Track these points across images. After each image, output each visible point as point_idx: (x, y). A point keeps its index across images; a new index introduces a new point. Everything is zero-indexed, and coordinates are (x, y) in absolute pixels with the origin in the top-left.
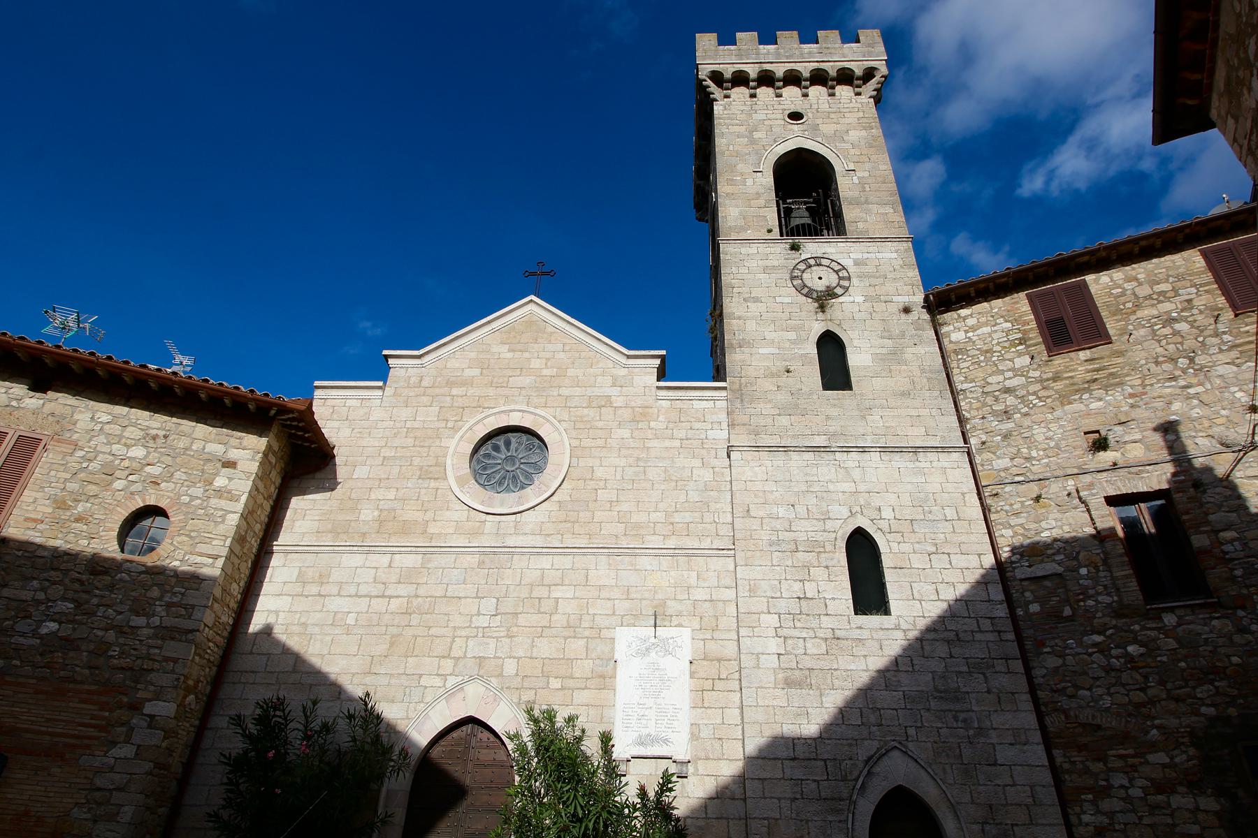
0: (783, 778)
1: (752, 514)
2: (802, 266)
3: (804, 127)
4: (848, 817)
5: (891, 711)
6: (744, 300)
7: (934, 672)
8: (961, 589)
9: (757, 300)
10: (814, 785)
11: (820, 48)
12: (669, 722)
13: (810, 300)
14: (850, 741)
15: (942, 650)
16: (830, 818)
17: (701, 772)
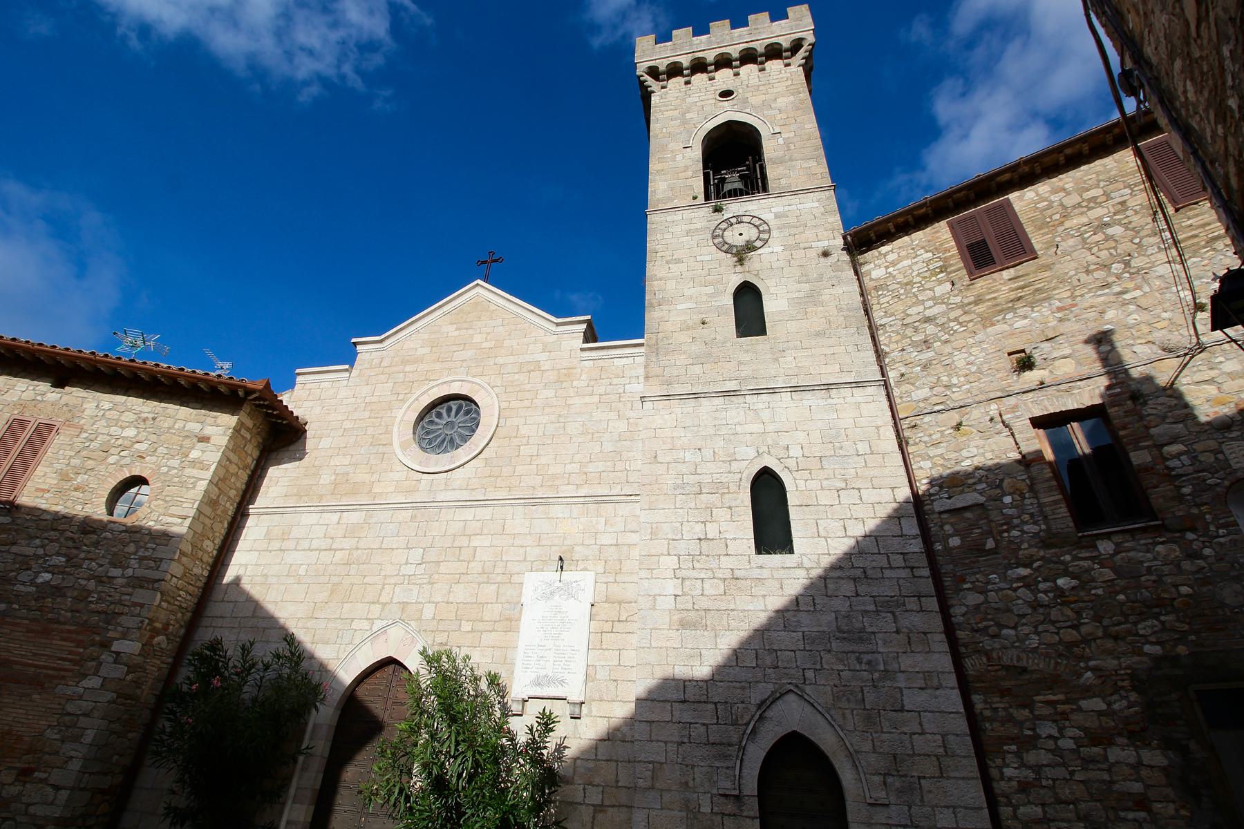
0: (671, 721)
1: (659, 459)
3: (734, 102)
5: (789, 653)
6: (667, 262)
8: (871, 525)
9: (679, 261)
10: (703, 729)
13: (729, 255)
14: (743, 684)
15: (848, 588)
16: (718, 765)
17: (594, 713)
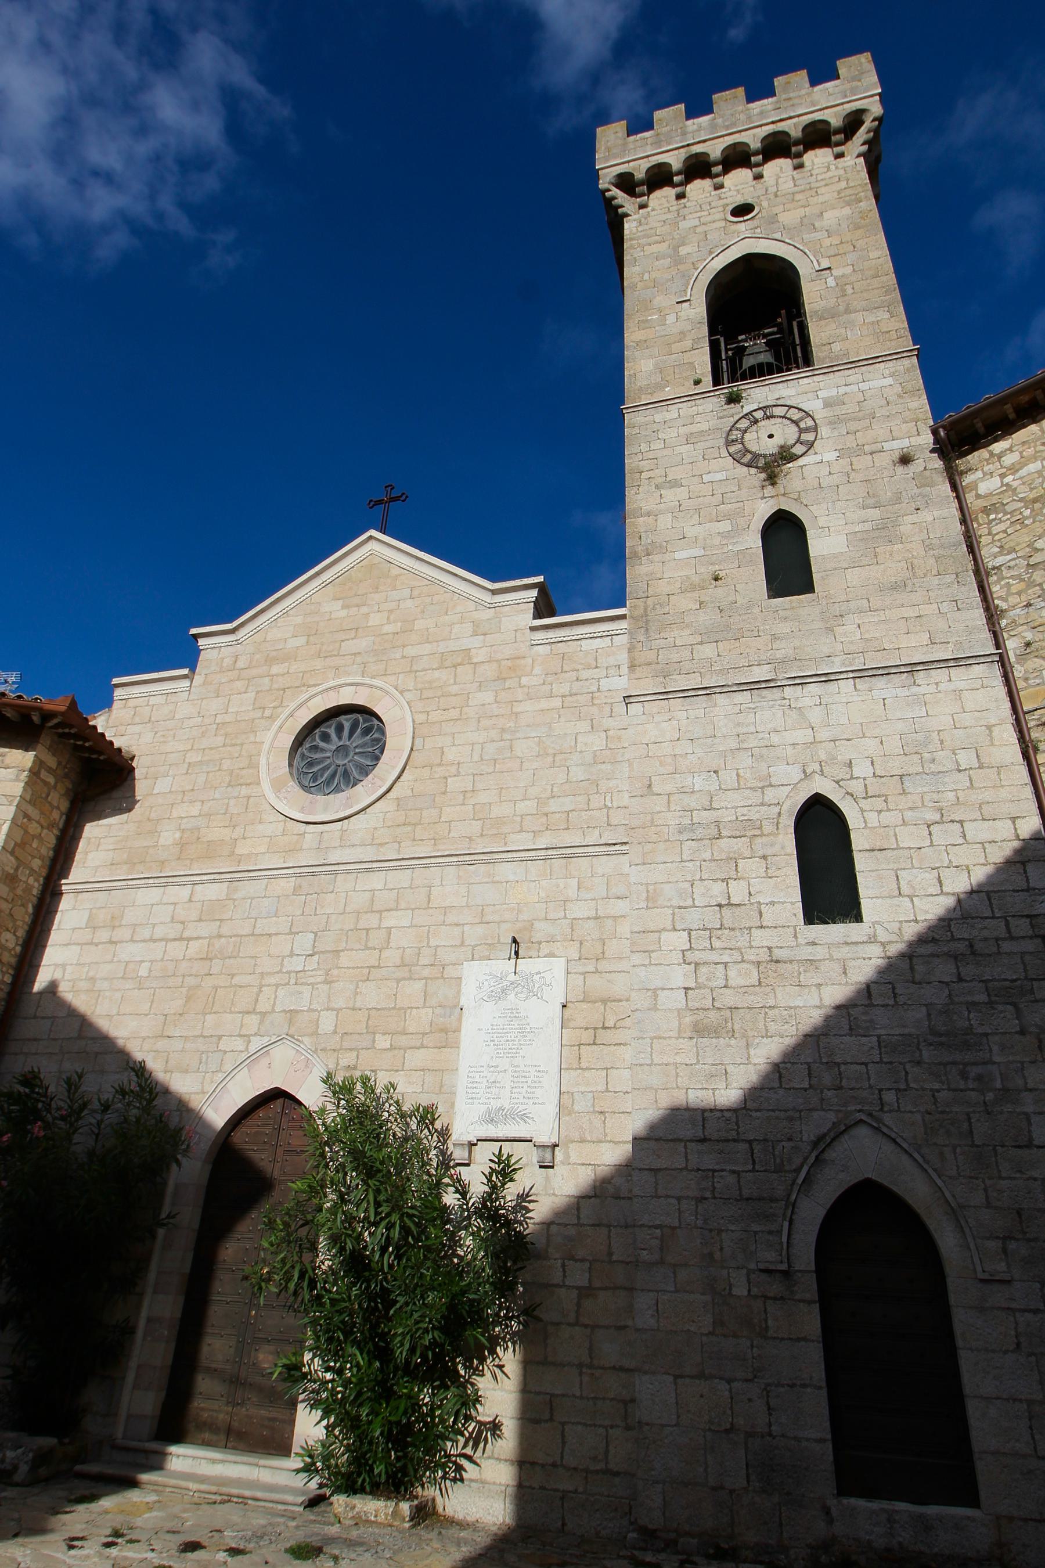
0: (686, 1168)
1: (656, 789)
2: (744, 424)
3: (755, 222)
4: (782, 1226)
5: (858, 1067)
6: (657, 487)
7: (931, 1004)
8: (980, 874)
9: (675, 484)
10: (732, 1179)
11: (777, 102)
12: (529, 1090)
13: (753, 471)
14: (790, 1113)
15: (945, 970)
16: (755, 1227)
17: (573, 1159)
